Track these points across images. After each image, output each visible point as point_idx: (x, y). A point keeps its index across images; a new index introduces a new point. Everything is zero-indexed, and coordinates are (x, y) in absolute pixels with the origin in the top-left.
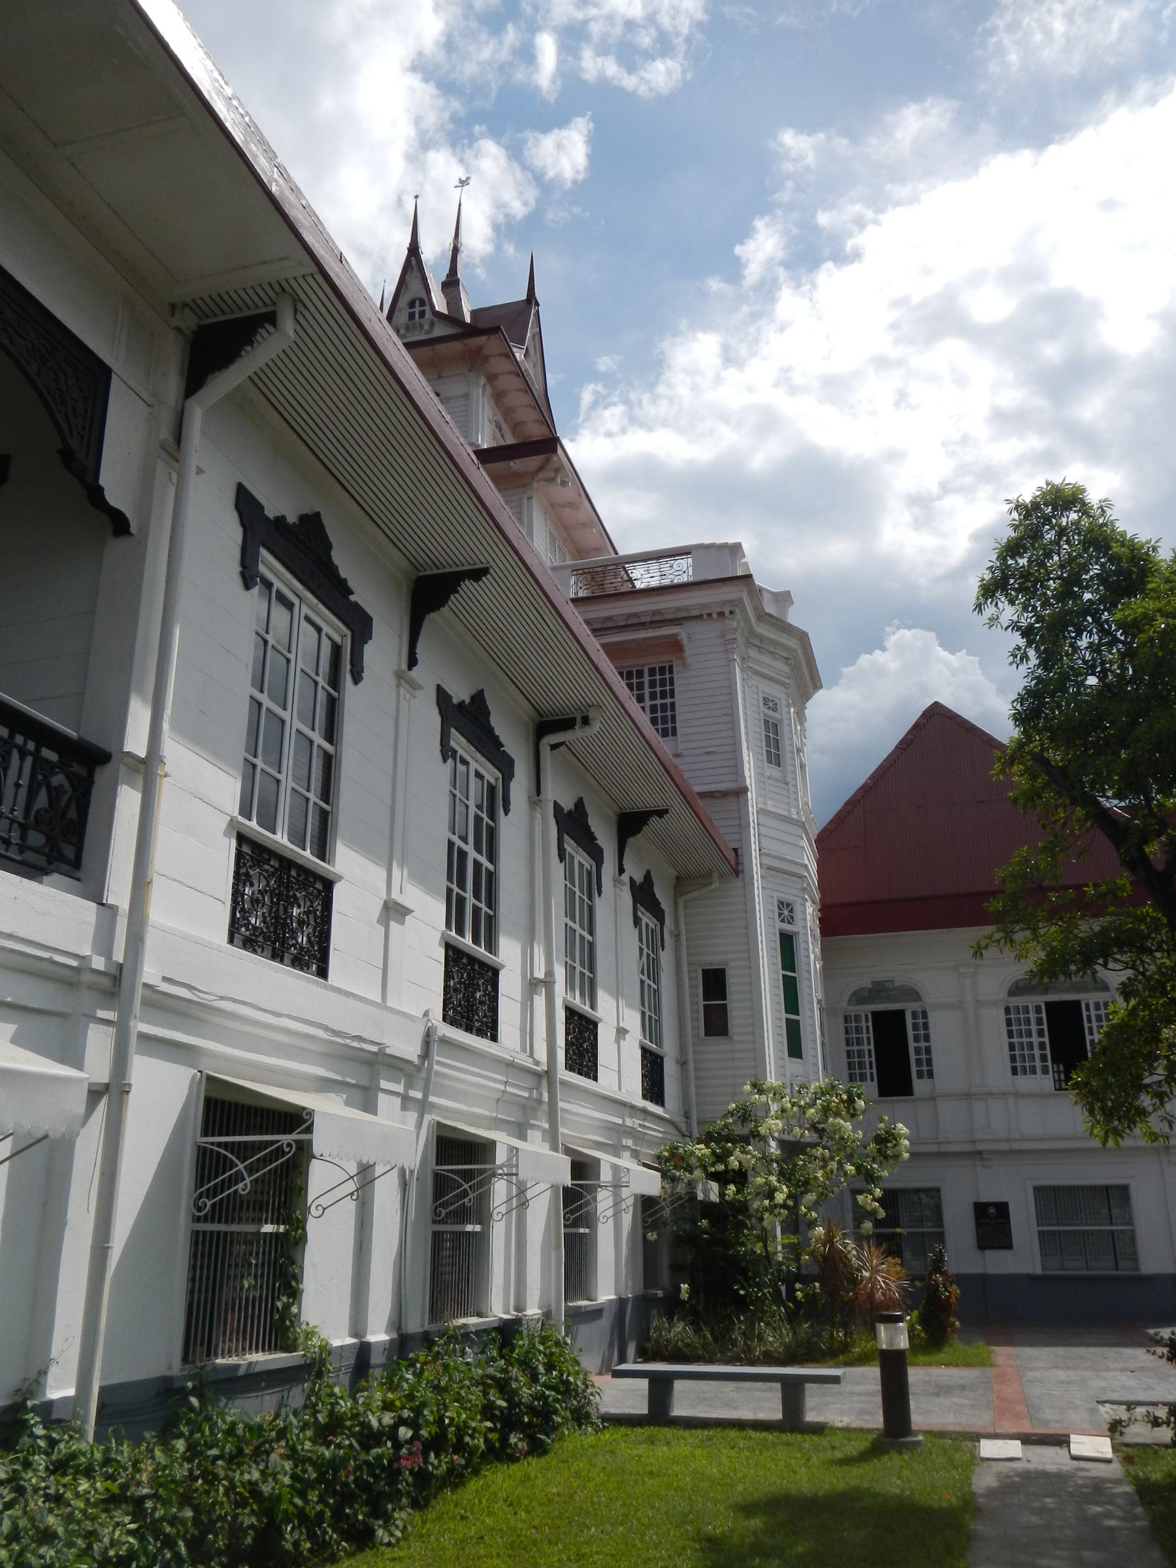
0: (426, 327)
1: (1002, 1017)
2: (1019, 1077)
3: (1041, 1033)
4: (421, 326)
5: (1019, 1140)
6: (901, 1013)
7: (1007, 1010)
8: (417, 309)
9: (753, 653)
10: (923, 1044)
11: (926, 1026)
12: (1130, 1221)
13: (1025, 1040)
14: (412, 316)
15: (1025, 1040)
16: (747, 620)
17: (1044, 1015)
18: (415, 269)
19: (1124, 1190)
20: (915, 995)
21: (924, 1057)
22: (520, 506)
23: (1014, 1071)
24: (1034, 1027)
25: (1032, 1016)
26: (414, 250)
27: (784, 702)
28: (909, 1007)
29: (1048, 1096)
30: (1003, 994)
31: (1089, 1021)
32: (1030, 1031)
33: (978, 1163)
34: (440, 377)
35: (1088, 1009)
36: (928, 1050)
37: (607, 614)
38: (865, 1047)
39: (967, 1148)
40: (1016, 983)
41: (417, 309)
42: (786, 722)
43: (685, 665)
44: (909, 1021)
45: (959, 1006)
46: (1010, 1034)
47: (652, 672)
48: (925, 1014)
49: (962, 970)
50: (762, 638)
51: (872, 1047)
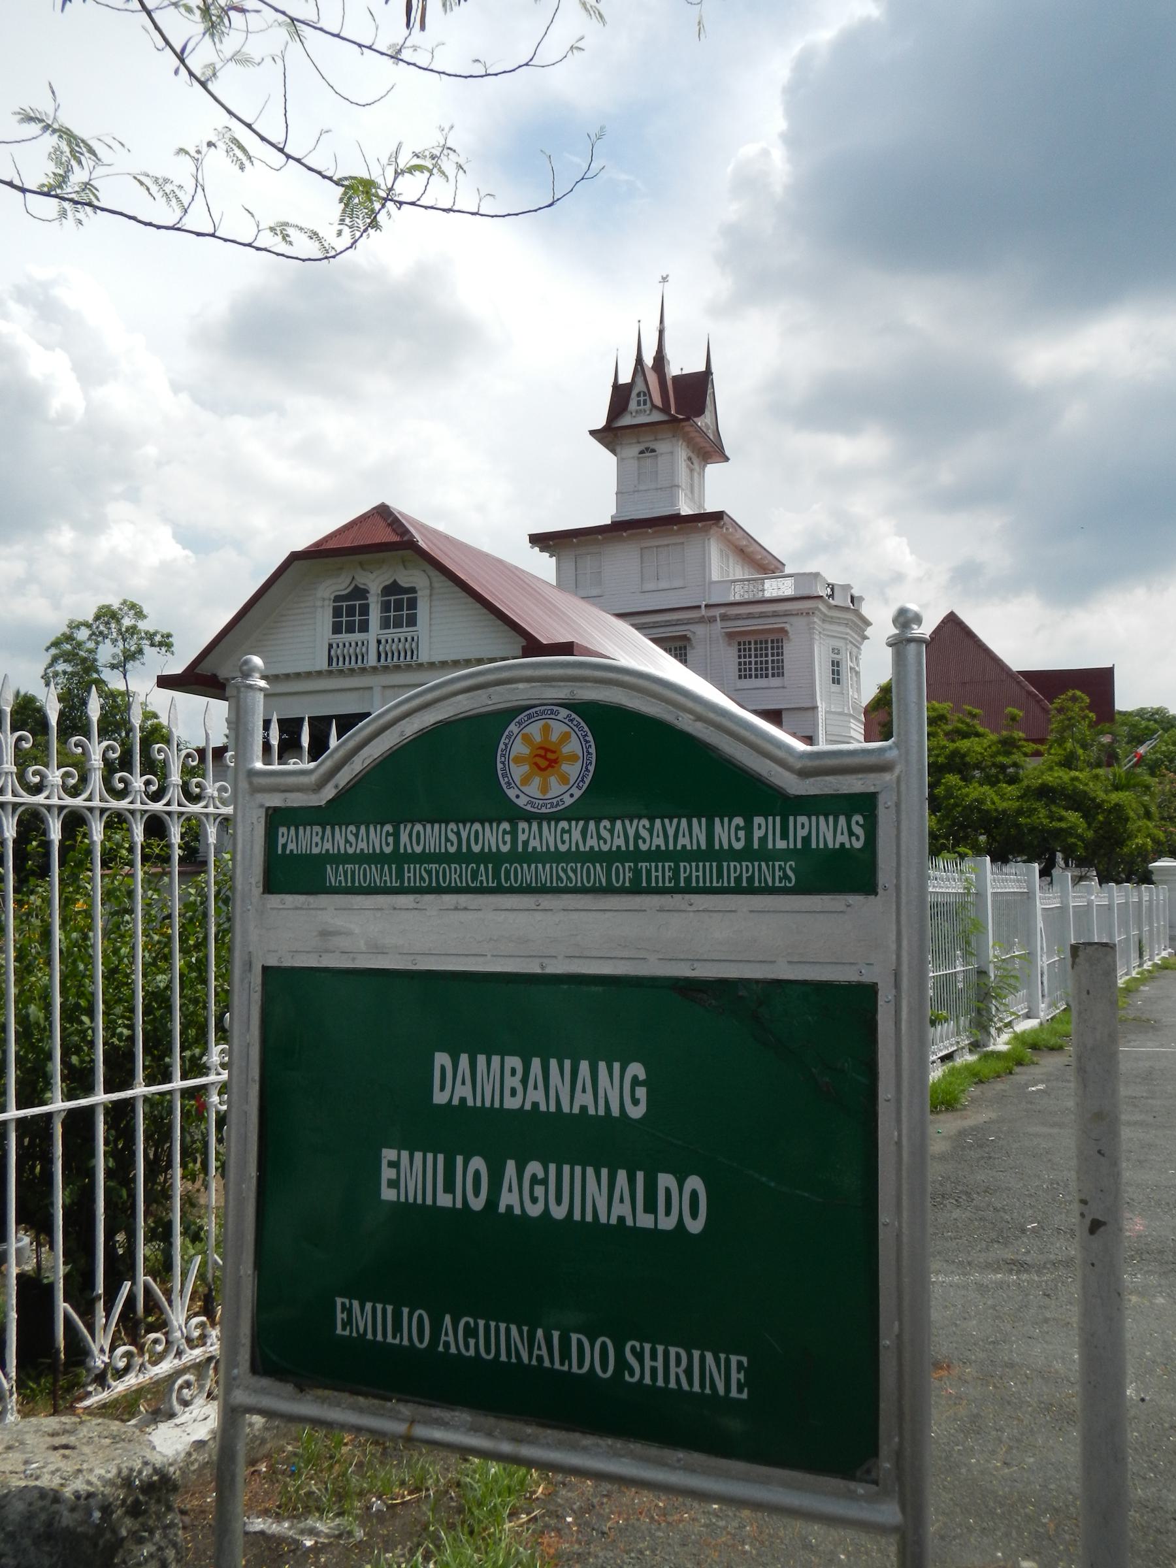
0: (648, 412)
4: (645, 411)
8: (642, 398)
9: (827, 626)
14: (639, 404)
16: (822, 613)
18: (640, 374)
22: (704, 543)
26: (639, 360)
27: (844, 648)
34: (656, 440)
37: (751, 611)
41: (642, 398)
42: (844, 659)
43: (788, 639)
47: (772, 642)
50: (832, 617)
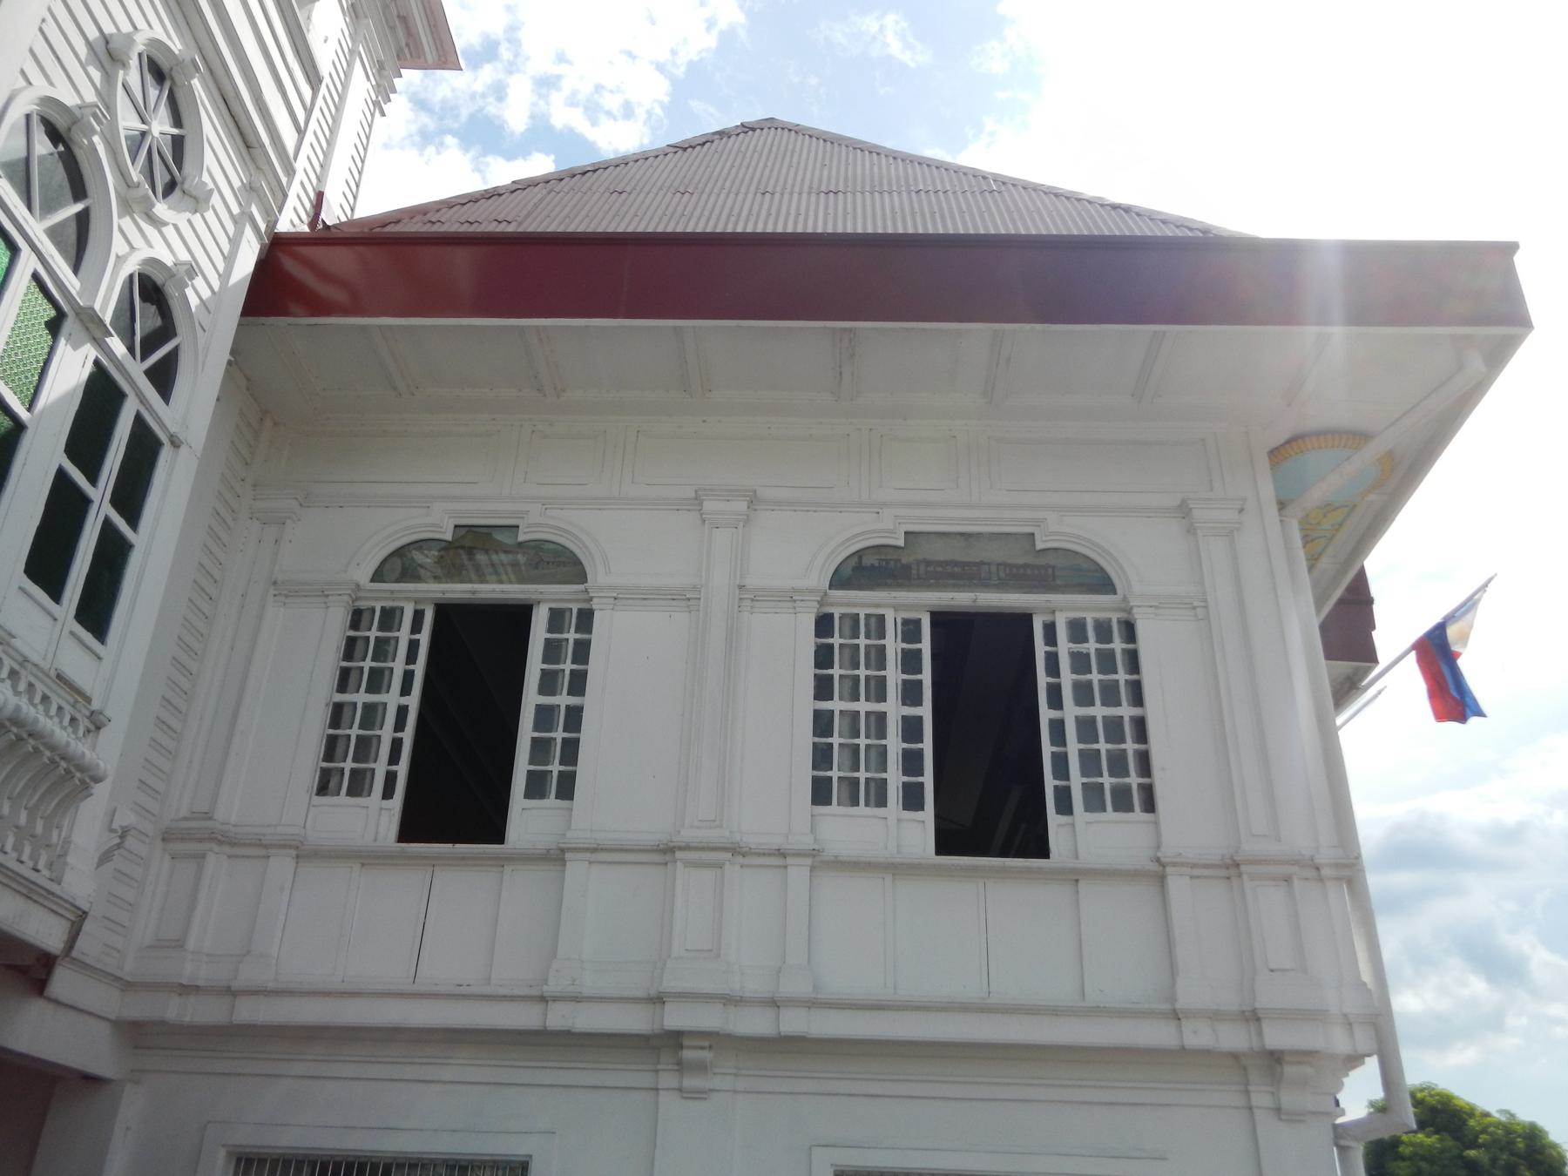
1: (808, 642)
3: (911, 694)
5: (813, 1004)
6: (519, 615)
7: (824, 625)
11: (582, 651)
13: (863, 706)
15: (863, 706)
17: (925, 646)
20: (566, 566)
23: (821, 792)
24: (894, 676)
25: (893, 646)
28: (546, 597)
30: (819, 578)
32: (882, 682)
33: (668, 1080)
36: (574, 717)
38: (391, 699)
39: (634, 1021)
40: (859, 554)
44: (539, 634)
46: (823, 689)
48: (586, 619)
51: (413, 701)
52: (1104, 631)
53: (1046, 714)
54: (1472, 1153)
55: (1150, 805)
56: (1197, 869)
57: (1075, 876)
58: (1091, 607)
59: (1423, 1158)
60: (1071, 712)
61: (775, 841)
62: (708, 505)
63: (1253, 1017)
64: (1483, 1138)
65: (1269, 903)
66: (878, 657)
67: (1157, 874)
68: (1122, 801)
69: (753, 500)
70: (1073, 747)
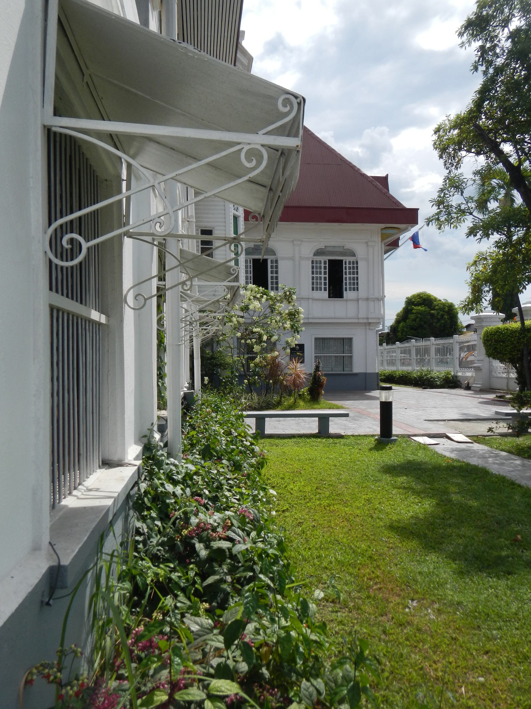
1: (311, 265)
2: (315, 291)
3: (325, 273)
5: (313, 318)
6: (265, 261)
7: (313, 262)
10: (275, 275)
11: (277, 267)
12: (351, 351)
13: (318, 276)
15: (318, 276)
19: (350, 339)
20: (273, 253)
21: (275, 281)
23: (313, 289)
24: (323, 270)
25: (323, 265)
28: (270, 258)
29: (326, 300)
31: (346, 269)
35: (346, 264)
36: (277, 278)
40: (317, 250)
45: (293, 259)
46: (313, 273)
48: (277, 261)
49: (295, 242)
51: (252, 275)
52: (353, 263)
53: (344, 276)
54: (433, 312)
55: (358, 290)
56: (363, 299)
57: (347, 300)
58: (352, 259)
59: (419, 313)
60: (348, 276)
61: (307, 297)
62: (295, 242)
63: (368, 318)
64: (437, 307)
65: (371, 304)
66: (320, 267)
67: (358, 300)
68: (354, 290)
69: (302, 241)
70: (348, 281)
